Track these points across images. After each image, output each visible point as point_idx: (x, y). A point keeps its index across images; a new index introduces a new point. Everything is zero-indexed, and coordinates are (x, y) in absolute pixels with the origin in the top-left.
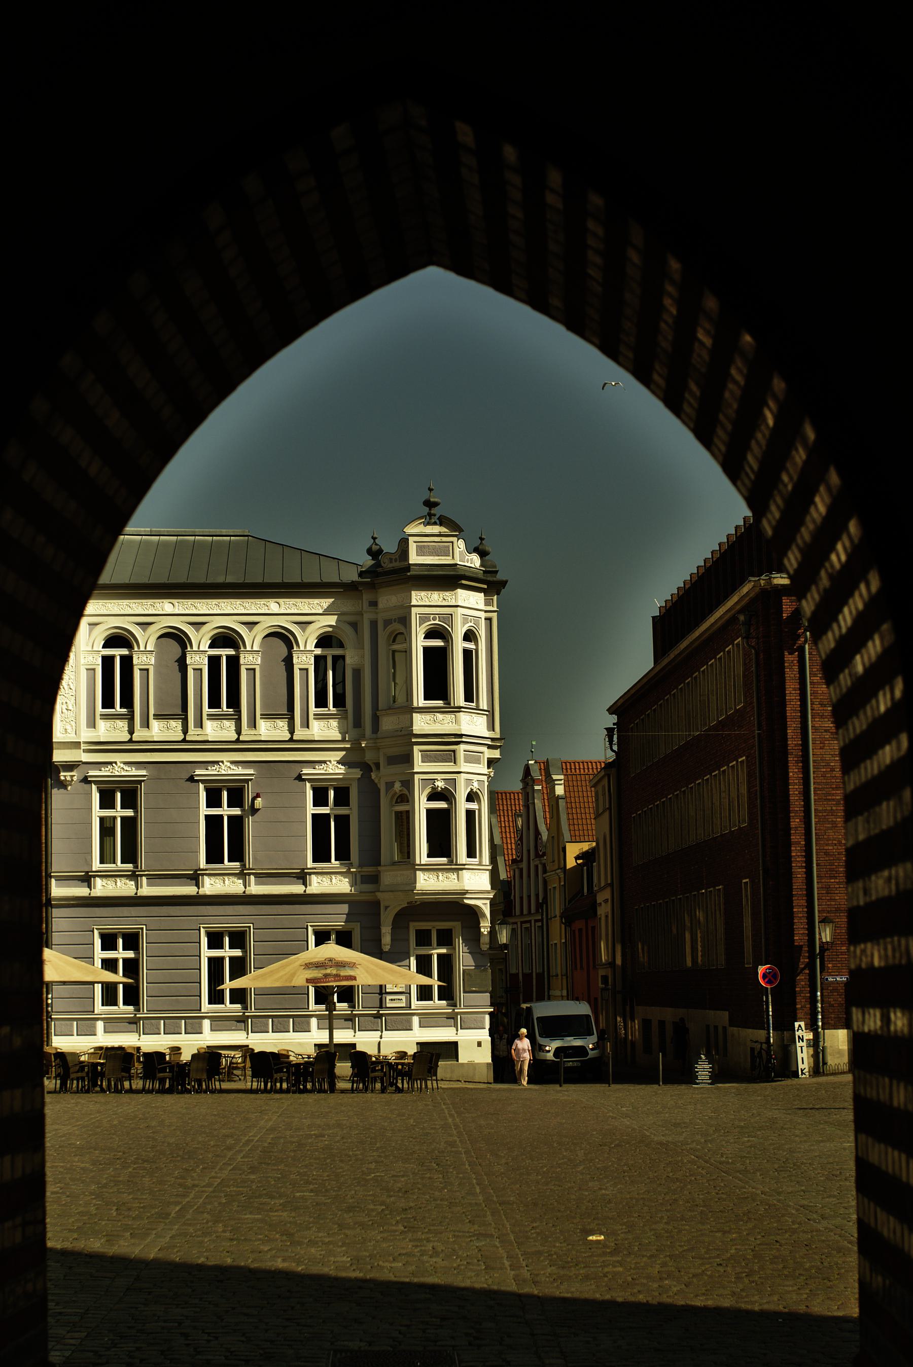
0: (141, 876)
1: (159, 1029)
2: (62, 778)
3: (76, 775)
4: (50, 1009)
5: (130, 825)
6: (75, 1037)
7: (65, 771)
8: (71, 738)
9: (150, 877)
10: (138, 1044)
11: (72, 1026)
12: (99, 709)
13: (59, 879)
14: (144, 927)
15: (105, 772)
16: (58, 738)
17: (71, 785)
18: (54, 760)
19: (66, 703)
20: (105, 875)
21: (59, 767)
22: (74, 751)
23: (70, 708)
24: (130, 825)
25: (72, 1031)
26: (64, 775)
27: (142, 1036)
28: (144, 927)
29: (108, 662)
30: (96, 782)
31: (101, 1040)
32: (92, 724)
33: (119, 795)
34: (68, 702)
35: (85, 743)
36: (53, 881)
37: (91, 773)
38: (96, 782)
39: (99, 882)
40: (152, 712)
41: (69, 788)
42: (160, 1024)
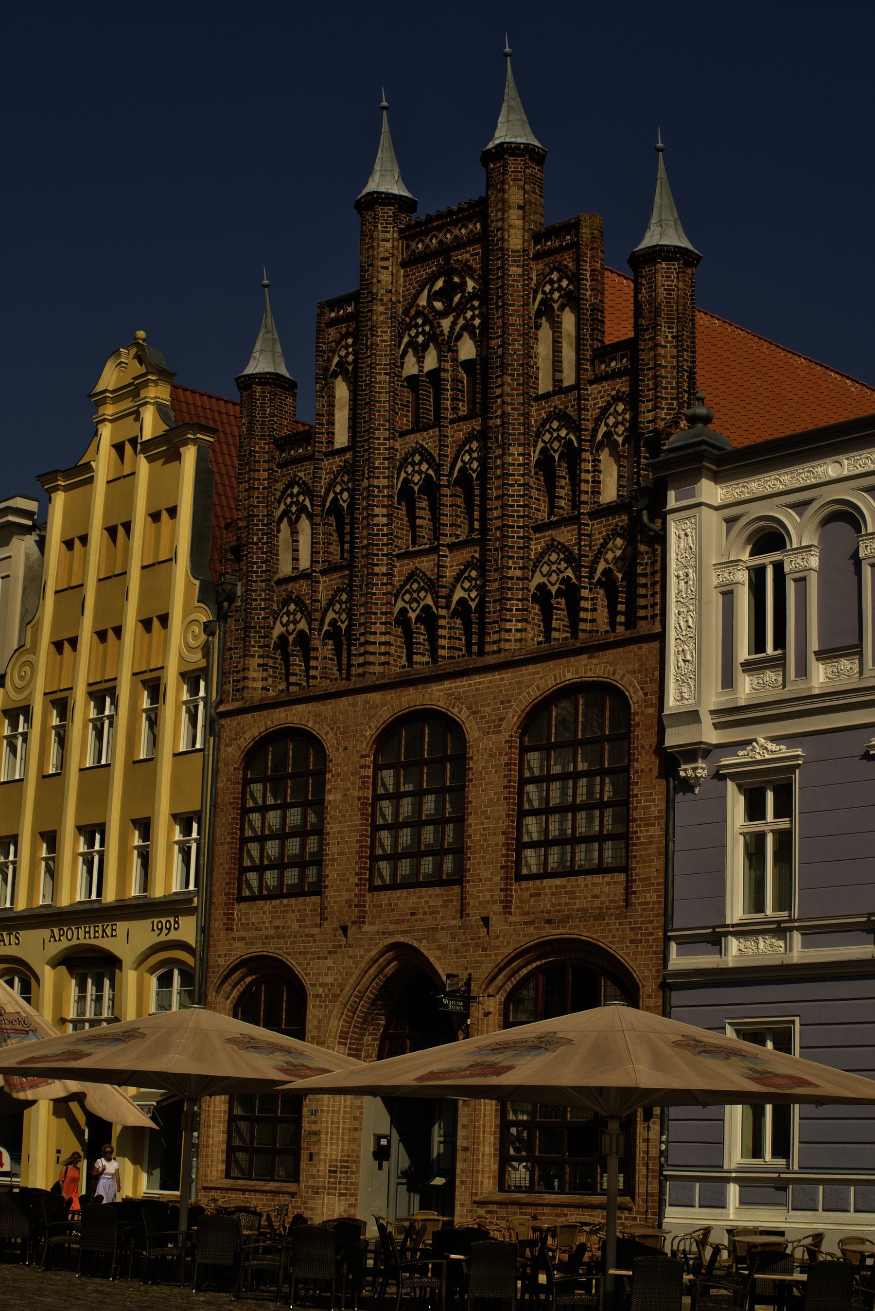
0: (791, 929)
1: (815, 1200)
2: (682, 774)
3: (701, 769)
4: (663, 1159)
5: (784, 839)
6: (820, 1213)
7: (686, 763)
8: (689, 704)
9: (806, 932)
10: (782, 1226)
11: (693, 1190)
12: (743, 653)
13: (682, 941)
14: (797, 1020)
15: (742, 756)
16: (671, 708)
17: (699, 785)
18: (666, 745)
19: (683, 650)
20: (744, 932)
21: (676, 755)
22: (692, 726)
23: (689, 657)
24: (784, 839)
25: (693, 1199)
26: (685, 770)
27: (792, 1213)
28: (797, 1020)
29: (757, 576)
30: (733, 777)
31: (731, 1217)
32: (728, 681)
33: (770, 796)
34: (686, 647)
35: (712, 712)
36: (673, 947)
37: (725, 762)
38: (733, 777)
39: (734, 945)
40: (814, 644)
41: (697, 790)
42: (817, 1193)
